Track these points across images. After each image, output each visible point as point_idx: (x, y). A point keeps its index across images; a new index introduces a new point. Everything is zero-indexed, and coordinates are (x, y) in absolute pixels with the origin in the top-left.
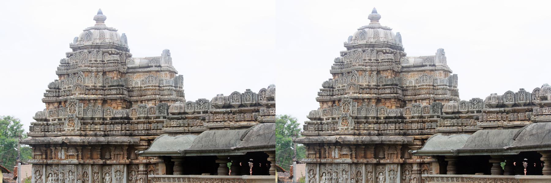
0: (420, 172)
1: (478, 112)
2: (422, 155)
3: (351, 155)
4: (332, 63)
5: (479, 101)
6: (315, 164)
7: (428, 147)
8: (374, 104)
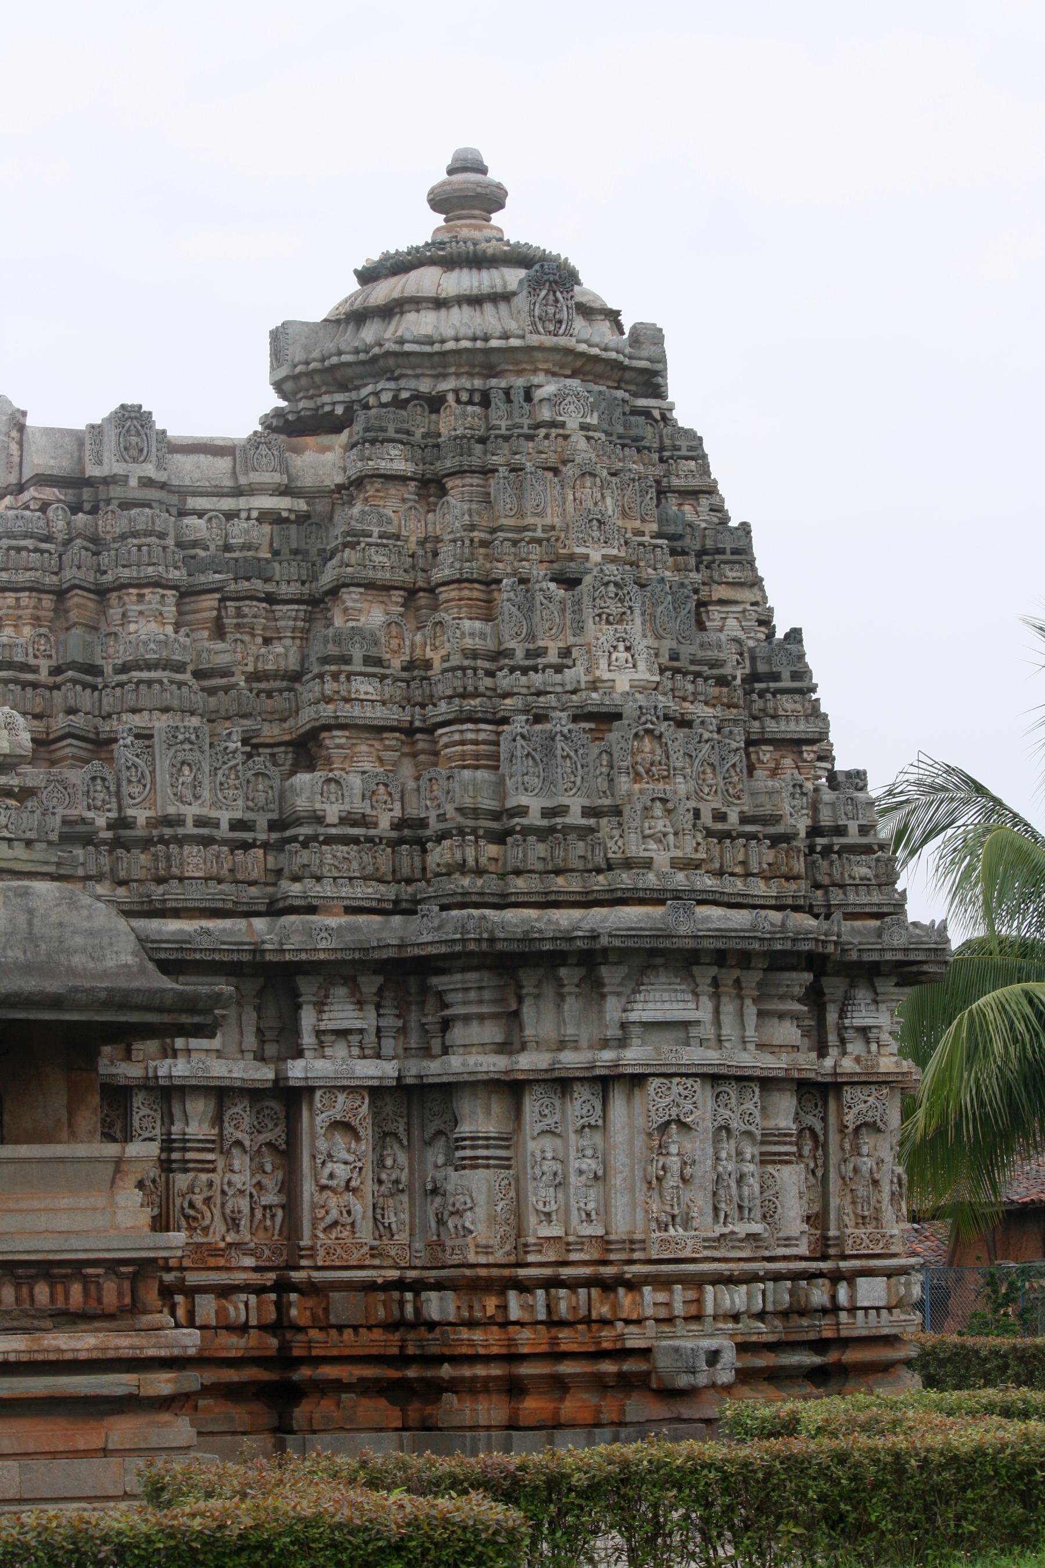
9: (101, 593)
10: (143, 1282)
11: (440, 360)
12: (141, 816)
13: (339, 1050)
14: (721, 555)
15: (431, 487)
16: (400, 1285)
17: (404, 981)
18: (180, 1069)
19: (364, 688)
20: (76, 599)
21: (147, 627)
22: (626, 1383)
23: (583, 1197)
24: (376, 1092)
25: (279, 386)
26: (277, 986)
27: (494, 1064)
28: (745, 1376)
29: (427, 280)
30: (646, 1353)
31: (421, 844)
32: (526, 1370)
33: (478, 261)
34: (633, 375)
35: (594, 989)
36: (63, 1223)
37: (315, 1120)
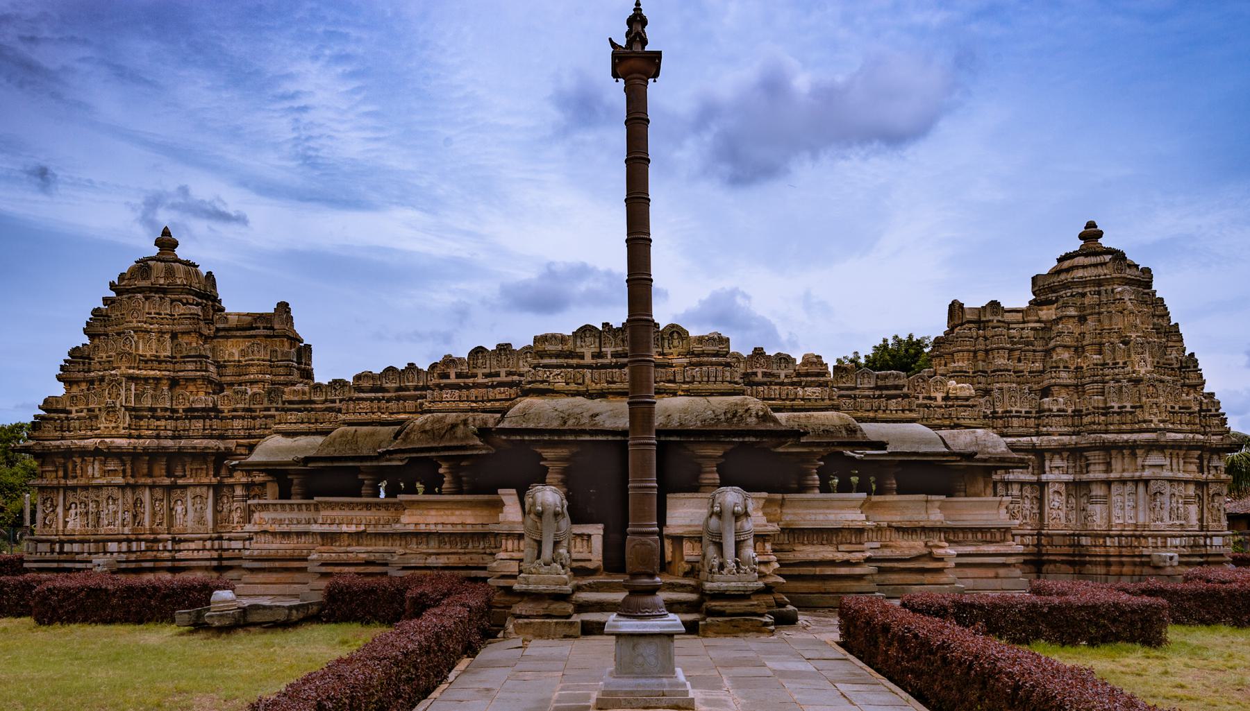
0: (248, 497)
1: (341, 401)
2: (250, 469)
3: (124, 471)
6: (56, 488)
8: (165, 388)
9: (987, 352)
12: (1000, 410)
13: (1056, 472)
16: (1074, 535)
17: (1075, 454)
18: (1011, 477)
19: (1063, 374)
20: (980, 354)
22: (1143, 564)
23: (1129, 512)
24: (1067, 483)
25: (1034, 293)
26: (1039, 453)
27: (1103, 476)
28: (1180, 563)
30: (1149, 556)
31: (1081, 416)
32: (1111, 559)
36: (985, 517)
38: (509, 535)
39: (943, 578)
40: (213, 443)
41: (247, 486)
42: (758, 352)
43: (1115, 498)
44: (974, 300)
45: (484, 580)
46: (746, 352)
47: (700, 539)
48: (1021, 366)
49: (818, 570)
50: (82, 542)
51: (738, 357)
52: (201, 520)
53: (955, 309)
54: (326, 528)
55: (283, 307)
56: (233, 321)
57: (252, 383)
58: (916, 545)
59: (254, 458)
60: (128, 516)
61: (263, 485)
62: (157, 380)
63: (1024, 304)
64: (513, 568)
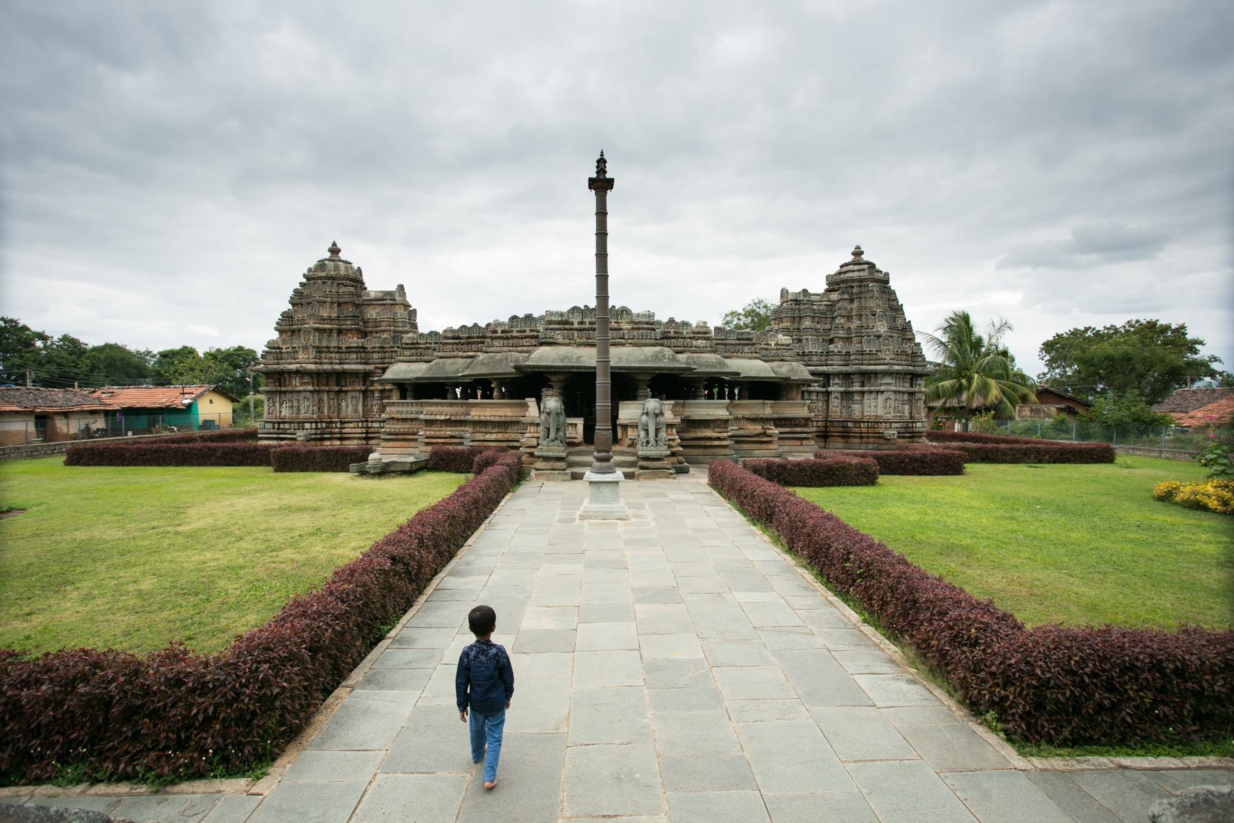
0: (382, 398)
2: (383, 382)
4: (291, 293)
5: (436, 334)
6: (275, 392)
7: (388, 375)
10: (806, 421)
11: (853, 280)
14: (898, 309)
15: (852, 301)
17: (846, 376)
21: (807, 323)
23: (873, 409)
26: (827, 376)
29: (851, 267)
33: (860, 264)
34: (884, 281)
35: (876, 377)
37: (833, 396)
38: (531, 424)
39: (771, 446)
40: (361, 367)
41: (382, 391)
42: (672, 321)
43: (866, 401)
44: (795, 289)
45: (518, 448)
46: (665, 320)
47: (637, 427)
48: (819, 326)
49: (702, 443)
50: (290, 423)
51: (659, 323)
52: (356, 411)
53: (784, 293)
54: (427, 417)
55: (401, 287)
56: (372, 295)
57: (383, 331)
58: (758, 428)
59: (388, 375)
60: (316, 408)
61: (390, 390)
62: (331, 330)
63: (822, 291)
64: (534, 442)
